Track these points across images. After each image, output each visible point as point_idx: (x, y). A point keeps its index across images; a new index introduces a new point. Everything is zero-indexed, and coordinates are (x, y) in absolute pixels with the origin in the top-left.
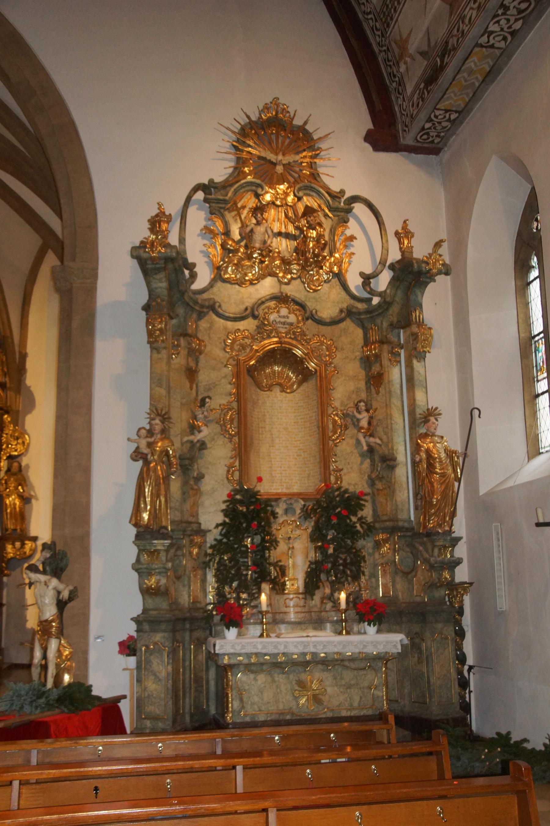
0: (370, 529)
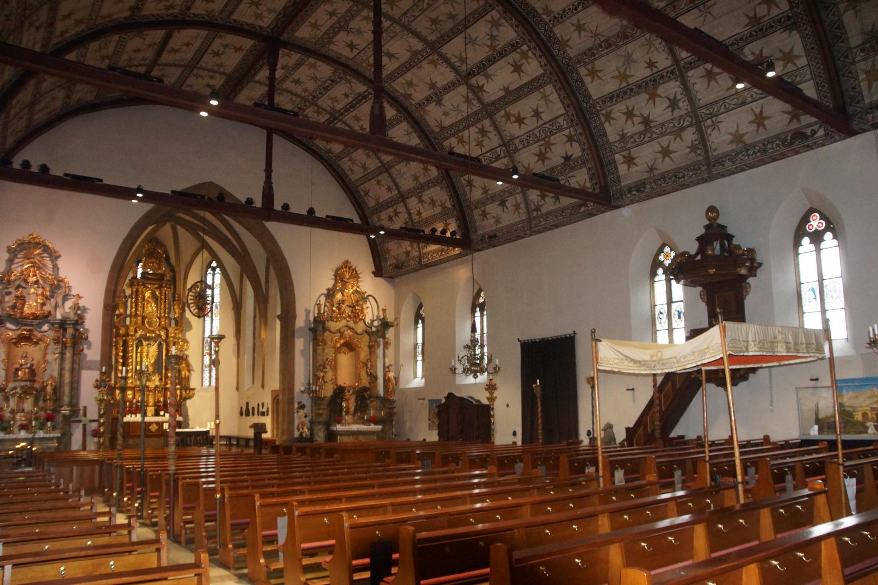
0: (370, 397)
